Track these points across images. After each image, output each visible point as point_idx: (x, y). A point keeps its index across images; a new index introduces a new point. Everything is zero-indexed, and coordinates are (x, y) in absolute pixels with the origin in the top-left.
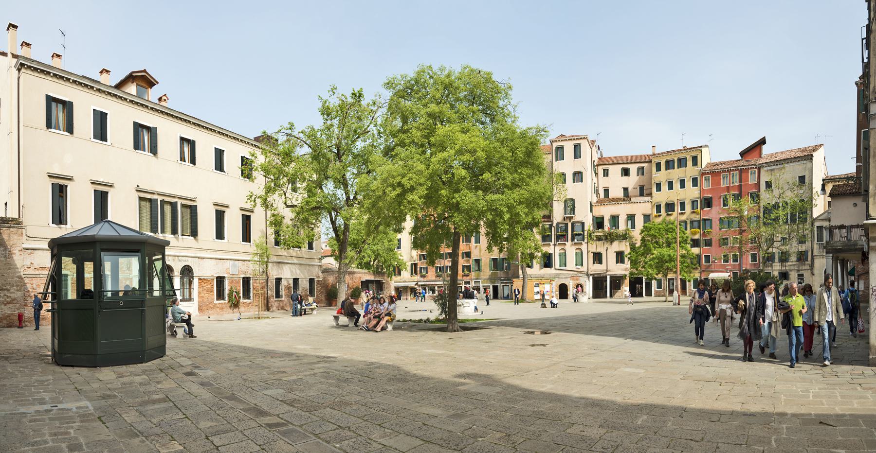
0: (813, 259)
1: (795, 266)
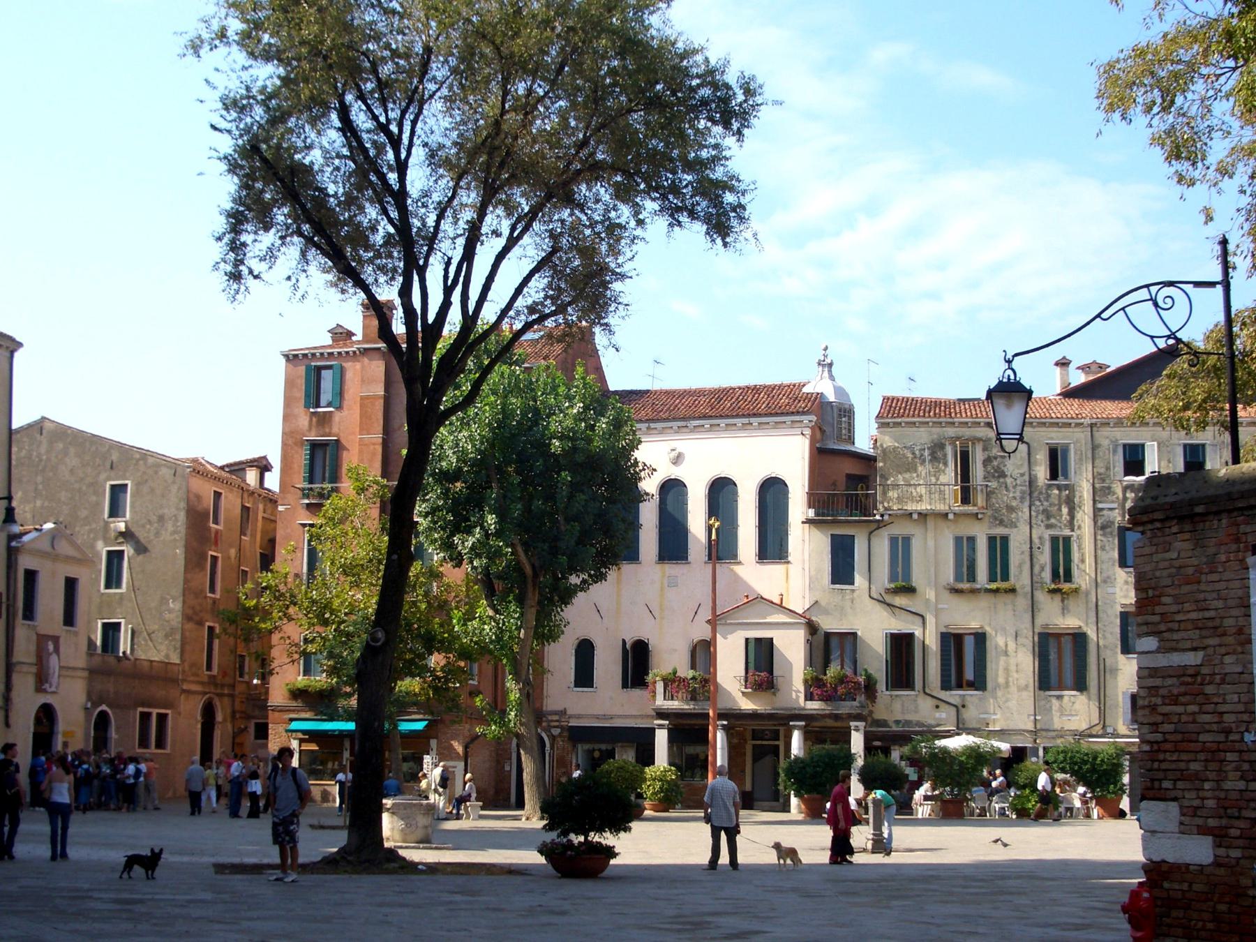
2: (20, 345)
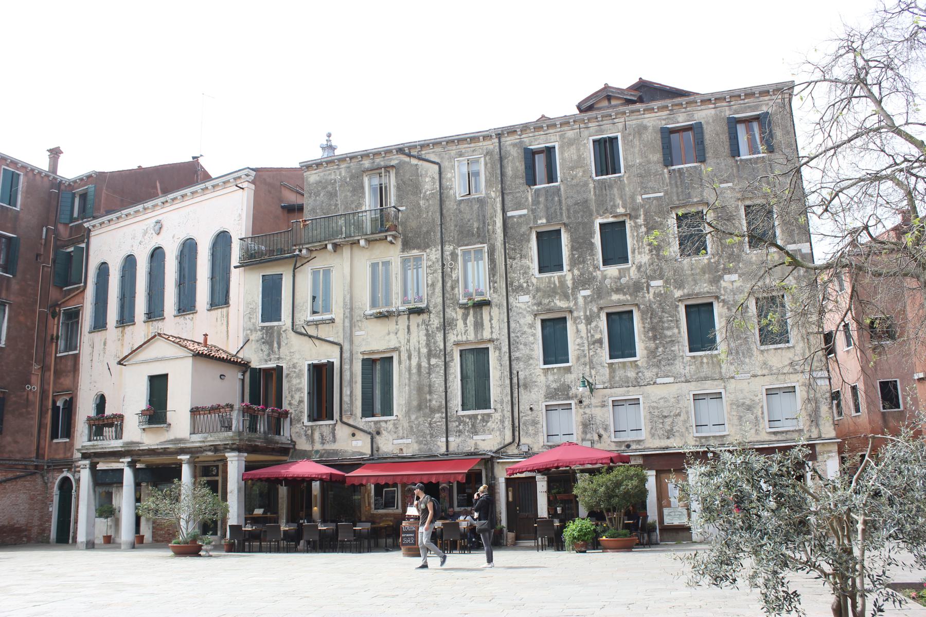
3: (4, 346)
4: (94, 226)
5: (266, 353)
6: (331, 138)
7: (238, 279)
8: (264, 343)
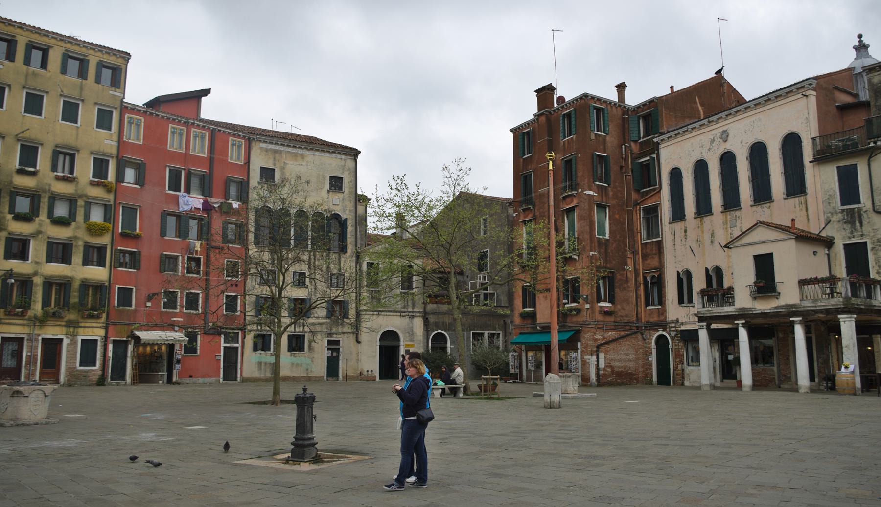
0: (358, 315)
1: (324, 326)
2: (360, 152)
3: (609, 238)
4: (662, 140)
5: (848, 231)
6: (862, 39)
7: (811, 173)
8: (845, 223)
